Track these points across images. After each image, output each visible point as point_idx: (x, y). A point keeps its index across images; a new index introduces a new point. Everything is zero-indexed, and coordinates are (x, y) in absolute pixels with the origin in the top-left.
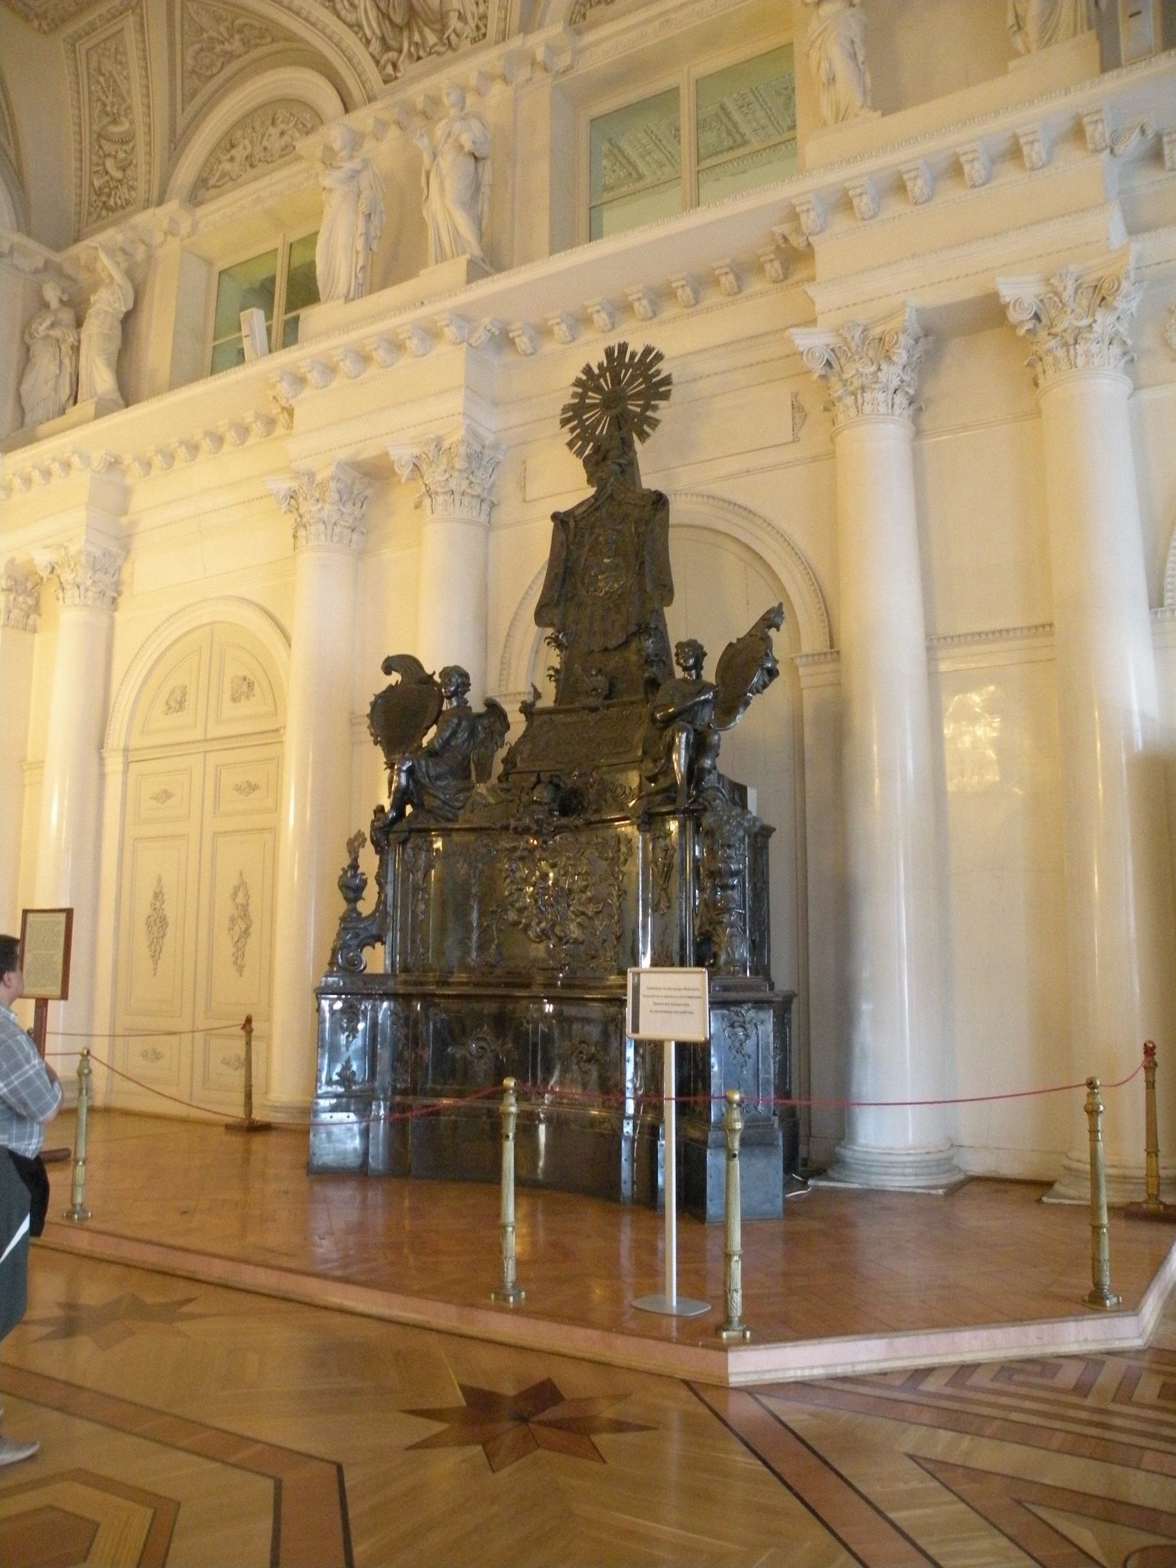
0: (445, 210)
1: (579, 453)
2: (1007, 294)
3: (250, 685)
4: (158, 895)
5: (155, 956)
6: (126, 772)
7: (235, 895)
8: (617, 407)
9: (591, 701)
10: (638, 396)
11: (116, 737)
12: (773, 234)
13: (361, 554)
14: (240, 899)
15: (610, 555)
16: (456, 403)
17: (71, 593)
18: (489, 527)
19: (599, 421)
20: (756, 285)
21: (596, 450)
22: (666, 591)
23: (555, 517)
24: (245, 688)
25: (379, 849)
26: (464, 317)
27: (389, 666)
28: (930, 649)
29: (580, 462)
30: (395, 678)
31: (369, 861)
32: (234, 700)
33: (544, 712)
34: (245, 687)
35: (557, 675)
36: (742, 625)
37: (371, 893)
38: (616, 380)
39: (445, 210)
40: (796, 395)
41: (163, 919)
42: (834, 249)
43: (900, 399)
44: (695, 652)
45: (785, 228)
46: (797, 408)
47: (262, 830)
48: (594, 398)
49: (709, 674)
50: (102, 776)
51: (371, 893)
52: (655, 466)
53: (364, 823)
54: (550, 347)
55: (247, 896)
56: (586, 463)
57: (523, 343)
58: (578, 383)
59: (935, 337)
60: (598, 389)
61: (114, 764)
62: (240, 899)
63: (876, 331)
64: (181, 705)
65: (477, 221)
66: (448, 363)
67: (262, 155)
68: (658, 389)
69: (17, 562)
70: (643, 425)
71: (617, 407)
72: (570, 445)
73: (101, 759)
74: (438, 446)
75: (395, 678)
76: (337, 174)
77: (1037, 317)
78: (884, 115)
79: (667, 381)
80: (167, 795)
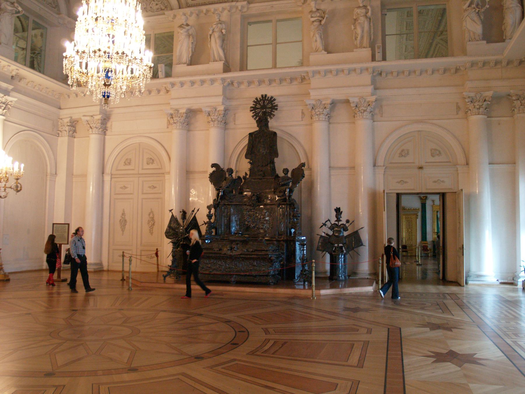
0: (215, 46)
1: (255, 119)
2: (351, 100)
3: (153, 160)
4: (123, 214)
5: (123, 231)
6: (111, 180)
7: (149, 215)
8: (264, 109)
9: (259, 177)
10: (269, 108)
11: (108, 170)
12: (301, 75)
13: (189, 131)
14: (151, 216)
15: (263, 144)
16: (220, 99)
17: (94, 130)
18: (225, 129)
19: (260, 112)
20: (295, 83)
21: (259, 119)
22: (277, 155)
23: (251, 134)
24: (151, 161)
25: (215, 208)
26: (223, 80)
27: (213, 165)
28: (330, 170)
29: (255, 121)
30: (214, 169)
31: (213, 211)
32: (148, 164)
33: (248, 179)
34: (151, 161)
35: (250, 170)
36: (296, 165)
37: (213, 217)
38: (264, 103)
39: (215, 46)
40: (302, 110)
41: (126, 221)
42: (315, 82)
43: (327, 117)
44: (286, 171)
45: (305, 74)
46: (303, 113)
47: (158, 199)
48: (258, 106)
49: (289, 175)
50: (103, 181)
51: (213, 217)
52: (273, 124)
53: (211, 202)
54: (242, 87)
55: (153, 215)
56: (257, 121)
57: (235, 84)
58: (254, 102)
59: (334, 104)
60: (260, 104)
61: (107, 178)
62: (151, 216)
63: (324, 102)
64: (129, 164)
65: (224, 50)
66: (218, 88)
67: (150, 9)
68: (274, 108)
69: (73, 118)
70: (271, 115)
71: (264, 109)
72: (253, 116)
73: (103, 176)
74: (216, 110)
75: (214, 169)
76: (184, 30)
77: (356, 106)
78: (328, 53)
79: (277, 106)
80: (125, 187)
